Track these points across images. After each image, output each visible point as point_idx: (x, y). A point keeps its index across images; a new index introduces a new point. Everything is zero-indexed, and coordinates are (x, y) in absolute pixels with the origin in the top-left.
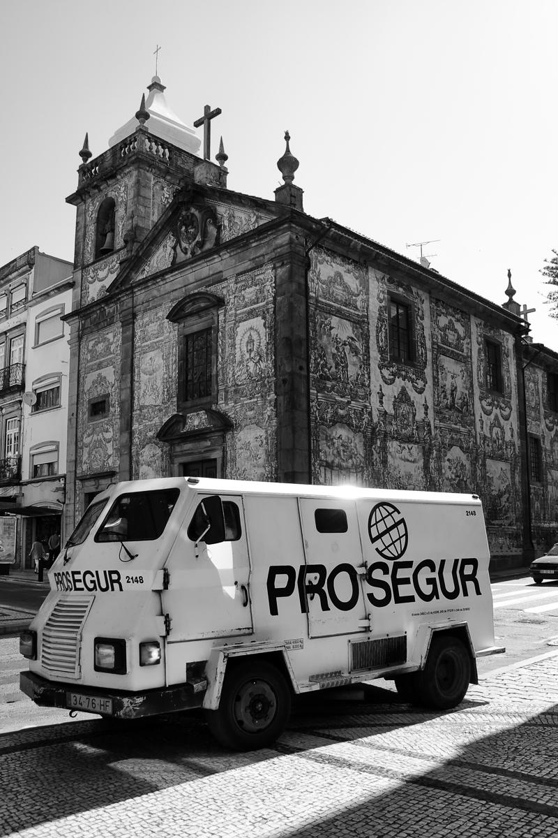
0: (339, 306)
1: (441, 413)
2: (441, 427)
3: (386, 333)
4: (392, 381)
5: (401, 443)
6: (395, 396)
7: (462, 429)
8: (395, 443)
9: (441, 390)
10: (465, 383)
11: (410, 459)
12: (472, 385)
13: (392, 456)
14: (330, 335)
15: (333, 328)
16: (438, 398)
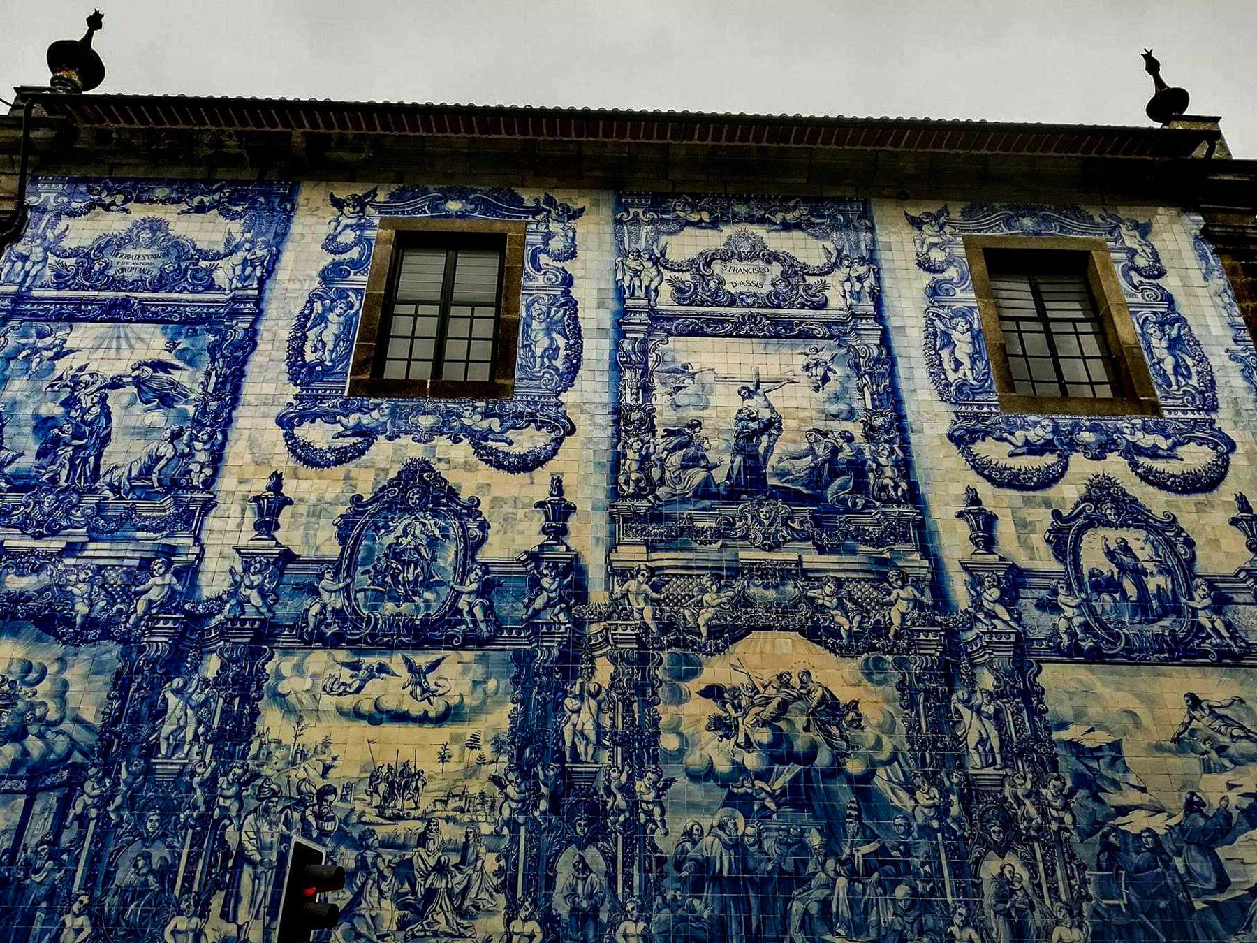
0: (121, 295)
1: (658, 518)
2: (652, 571)
3: (349, 320)
4: (342, 457)
5: (360, 652)
6: (357, 500)
7: (812, 559)
8: (319, 660)
9: (660, 442)
10: (837, 397)
11: (416, 709)
12: (892, 399)
13: (288, 710)
14: (52, 369)
15: (71, 351)
16: (640, 469)
